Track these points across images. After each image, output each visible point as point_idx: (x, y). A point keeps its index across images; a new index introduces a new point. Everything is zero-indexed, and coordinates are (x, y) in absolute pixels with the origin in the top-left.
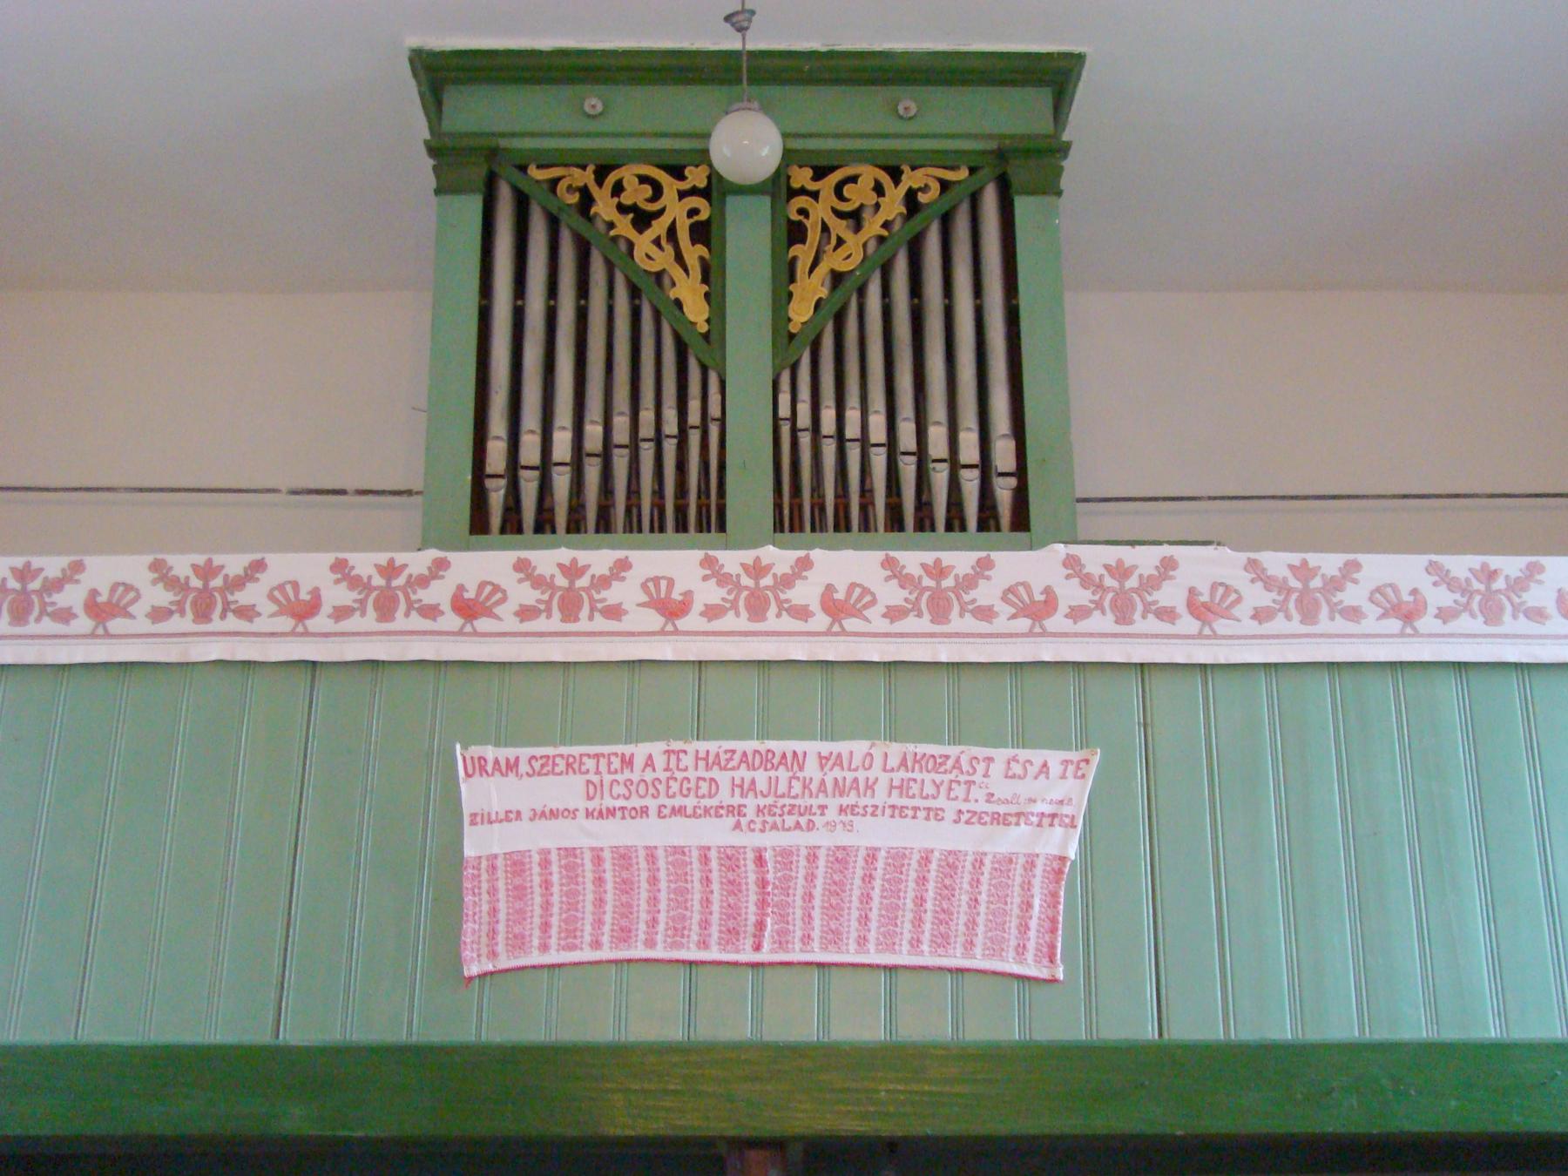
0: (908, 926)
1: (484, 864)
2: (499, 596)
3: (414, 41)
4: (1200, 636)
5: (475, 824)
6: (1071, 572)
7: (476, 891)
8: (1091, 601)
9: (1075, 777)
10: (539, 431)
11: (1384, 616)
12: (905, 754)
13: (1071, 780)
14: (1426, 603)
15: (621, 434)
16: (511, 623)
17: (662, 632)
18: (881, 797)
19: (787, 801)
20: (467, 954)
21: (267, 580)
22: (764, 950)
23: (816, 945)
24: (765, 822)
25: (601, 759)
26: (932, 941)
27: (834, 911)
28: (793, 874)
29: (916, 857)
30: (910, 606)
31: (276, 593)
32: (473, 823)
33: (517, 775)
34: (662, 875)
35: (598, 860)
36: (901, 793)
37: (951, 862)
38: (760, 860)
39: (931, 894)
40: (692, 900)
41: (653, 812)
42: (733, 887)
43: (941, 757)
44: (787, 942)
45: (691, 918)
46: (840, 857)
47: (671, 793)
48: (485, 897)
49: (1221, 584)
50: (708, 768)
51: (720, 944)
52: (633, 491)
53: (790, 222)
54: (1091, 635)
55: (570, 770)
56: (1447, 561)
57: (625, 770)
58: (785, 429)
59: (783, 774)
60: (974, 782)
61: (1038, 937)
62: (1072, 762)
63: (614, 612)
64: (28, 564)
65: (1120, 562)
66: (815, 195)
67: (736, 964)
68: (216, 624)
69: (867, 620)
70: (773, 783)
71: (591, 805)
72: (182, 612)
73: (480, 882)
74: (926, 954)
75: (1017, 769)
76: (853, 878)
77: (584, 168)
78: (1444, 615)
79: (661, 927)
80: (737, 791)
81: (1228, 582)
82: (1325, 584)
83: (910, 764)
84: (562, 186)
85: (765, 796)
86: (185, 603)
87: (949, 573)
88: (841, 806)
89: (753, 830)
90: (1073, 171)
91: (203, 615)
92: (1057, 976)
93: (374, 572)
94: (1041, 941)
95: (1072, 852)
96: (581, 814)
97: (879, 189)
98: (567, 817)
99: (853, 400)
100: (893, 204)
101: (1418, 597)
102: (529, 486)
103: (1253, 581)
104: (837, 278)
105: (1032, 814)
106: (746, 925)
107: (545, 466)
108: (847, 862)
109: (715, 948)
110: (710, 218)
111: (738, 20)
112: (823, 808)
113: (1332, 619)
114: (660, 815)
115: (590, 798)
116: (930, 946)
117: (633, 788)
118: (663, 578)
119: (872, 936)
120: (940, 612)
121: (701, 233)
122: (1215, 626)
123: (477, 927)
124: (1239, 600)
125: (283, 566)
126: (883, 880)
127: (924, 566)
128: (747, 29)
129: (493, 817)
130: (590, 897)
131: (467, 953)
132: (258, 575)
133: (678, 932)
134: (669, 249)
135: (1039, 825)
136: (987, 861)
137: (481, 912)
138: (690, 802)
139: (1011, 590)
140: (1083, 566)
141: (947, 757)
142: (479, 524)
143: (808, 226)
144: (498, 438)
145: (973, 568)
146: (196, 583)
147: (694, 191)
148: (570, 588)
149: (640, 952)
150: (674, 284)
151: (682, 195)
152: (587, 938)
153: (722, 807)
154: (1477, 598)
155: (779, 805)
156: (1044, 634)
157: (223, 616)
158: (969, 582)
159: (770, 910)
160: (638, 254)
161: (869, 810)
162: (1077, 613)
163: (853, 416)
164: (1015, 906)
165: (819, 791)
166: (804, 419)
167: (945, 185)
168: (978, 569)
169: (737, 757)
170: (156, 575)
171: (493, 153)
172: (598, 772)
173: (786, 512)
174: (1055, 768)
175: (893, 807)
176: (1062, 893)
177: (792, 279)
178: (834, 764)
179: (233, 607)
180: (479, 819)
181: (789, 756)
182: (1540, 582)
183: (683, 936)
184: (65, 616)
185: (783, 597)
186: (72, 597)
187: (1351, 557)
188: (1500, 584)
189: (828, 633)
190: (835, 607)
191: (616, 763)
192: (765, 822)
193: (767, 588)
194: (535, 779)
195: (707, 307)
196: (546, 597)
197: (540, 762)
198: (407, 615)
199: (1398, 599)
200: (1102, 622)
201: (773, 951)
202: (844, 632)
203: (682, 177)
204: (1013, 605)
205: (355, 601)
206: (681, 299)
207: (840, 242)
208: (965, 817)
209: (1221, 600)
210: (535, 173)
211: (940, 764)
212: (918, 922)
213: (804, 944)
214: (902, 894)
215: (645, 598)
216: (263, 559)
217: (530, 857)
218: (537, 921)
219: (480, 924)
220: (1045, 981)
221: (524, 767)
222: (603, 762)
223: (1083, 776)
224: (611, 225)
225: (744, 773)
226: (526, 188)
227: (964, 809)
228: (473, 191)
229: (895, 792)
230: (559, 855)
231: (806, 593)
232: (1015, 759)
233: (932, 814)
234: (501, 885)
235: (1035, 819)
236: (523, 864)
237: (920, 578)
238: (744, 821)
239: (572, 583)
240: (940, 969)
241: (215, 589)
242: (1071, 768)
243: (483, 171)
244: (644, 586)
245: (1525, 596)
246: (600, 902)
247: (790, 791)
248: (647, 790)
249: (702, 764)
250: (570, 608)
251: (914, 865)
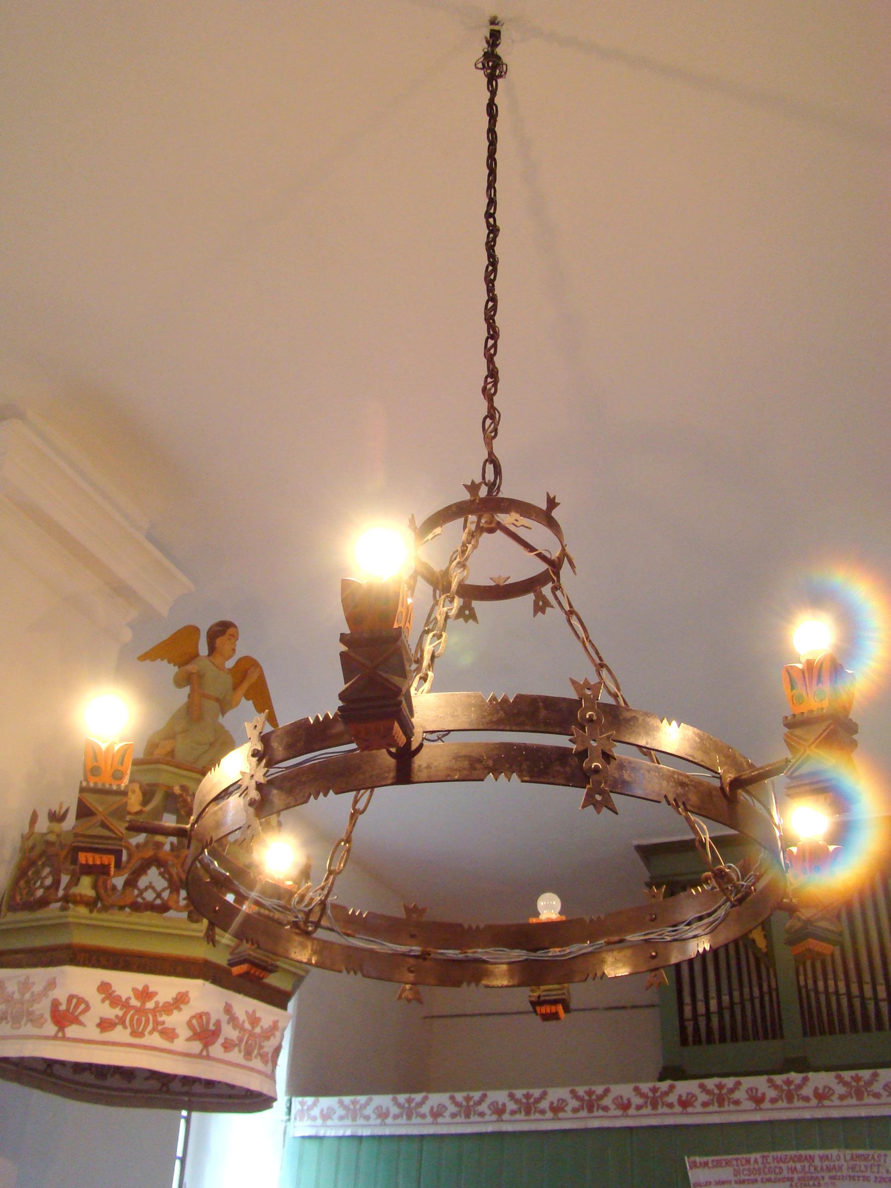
15: (737, 999)
19: (809, 1175)
24: (801, 1184)
50: (778, 1162)
63: (737, 1102)
68: (595, 1113)
69: (832, 1101)
70: (803, 1168)
71: (737, 1178)
80: (790, 1171)
91: (590, 1110)
96: (733, 1182)
112: (823, 1178)
114: (762, 1182)
120: (859, 1096)
127: (852, 1077)
138: (773, 1176)
141: (869, 1155)
158: (870, 1083)
175: (850, 1176)
181: (808, 1157)
191: (744, 1162)
192: (801, 1184)
202: (823, 1106)
221: (710, 1165)
222: (739, 1162)
225: (791, 1164)
231: (807, 1091)
238: (793, 1184)
244: (747, 1091)
250: (721, 1101)
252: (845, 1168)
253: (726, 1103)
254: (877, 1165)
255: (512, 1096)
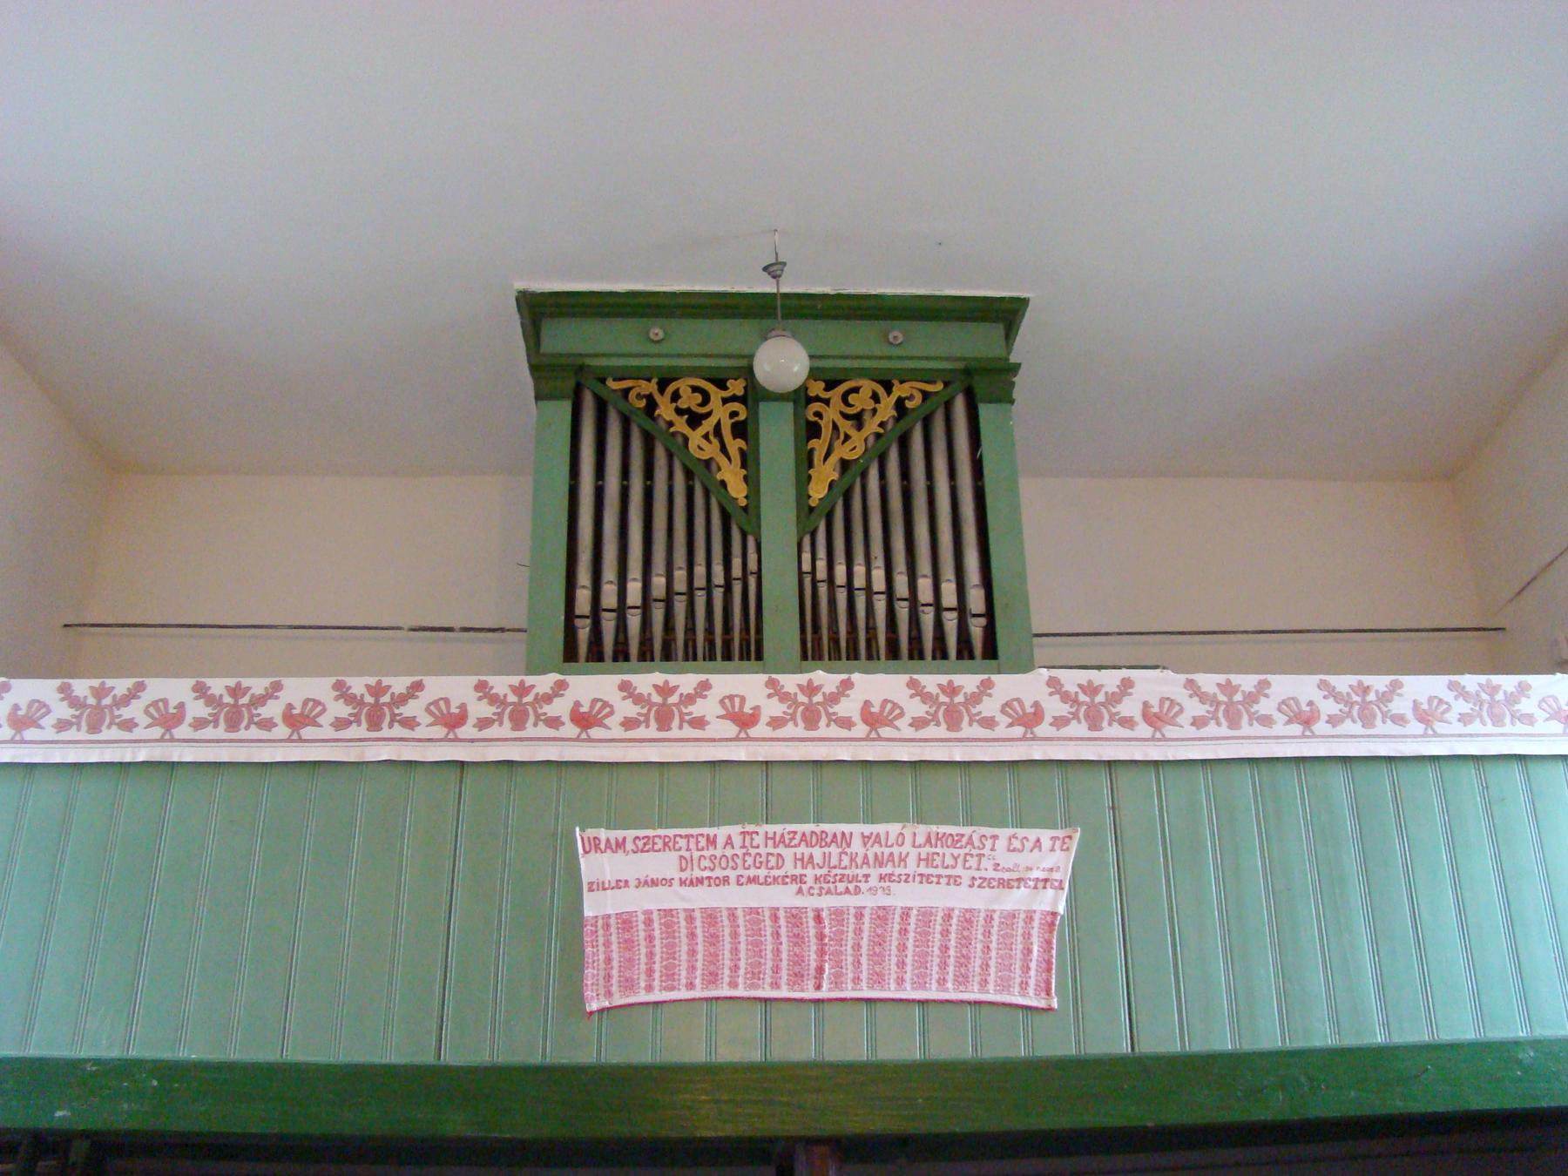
0: (936, 969)
1: (600, 922)
2: (608, 710)
3: (520, 285)
4: (1153, 739)
5: (593, 891)
6: (1053, 690)
7: (594, 943)
8: (1069, 713)
9: (1062, 850)
10: (616, 581)
11: (1290, 722)
12: (929, 833)
13: (1058, 852)
14: (1319, 711)
15: (680, 584)
16: (618, 732)
17: (737, 739)
18: (911, 867)
19: (839, 871)
20: (588, 993)
21: (425, 697)
22: (824, 989)
23: (864, 984)
24: (821, 888)
25: (691, 840)
26: (955, 980)
27: (877, 958)
28: (845, 929)
29: (941, 914)
30: (930, 718)
31: (432, 708)
32: (591, 890)
33: (624, 852)
34: (742, 930)
35: (690, 918)
36: (927, 864)
37: (968, 918)
38: (818, 919)
39: (953, 943)
40: (766, 950)
41: (733, 880)
42: (798, 939)
43: (957, 835)
44: (842, 983)
45: (765, 964)
46: (881, 914)
47: (746, 865)
48: (602, 949)
49: (1168, 699)
50: (775, 846)
51: (789, 985)
52: (690, 629)
53: (808, 422)
54: (1071, 739)
55: (667, 848)
56: (1333, 680)
57: (710, 848)
58: (808, 580)
59: (834, 850)
60: (984, 855)
61: (1037, 976)
62: (1058, 838)
63: (699, 723)
64: (239, 684)
65: (1090, 682)
66: (827, 402)
67: (802, 1000)
68: (386, 732)
70: (826, 857)
71: (684, 875)
72: (359, 723)
73: (597, 936)
74: (951, 990)
75: (1016, 844)
76: (891, 932)
77: (649, 380)
78: (1333, 721)
79: (742, 972)
80: (799, 864)
81: (1173, 698)
82: (1245, 698)
83: (933, 841)
84: (632, 395)
85: (821, 868)
86: (361, 715)
87: (960, 691)
88: (881, 875)
89: (812, 895)
90: (1022, 386)
91: (375, 724)
92: (1053, 1006)
93: (508, 691)
94: (1040, 978)
95: (1061, 908)
96: (676, 883)
97: (875, 397)
98: (665, 885)
99: (859, 557)
100: (887, 410)
101: (1314, 707)
102: (609, 624)
103: (1191, 696)
104: (845, 465)
105: (1030, 879)
106: (808, 970)
107: (622, 609)
108: (887, 919)
109: (784, 987)
110: (746, 419)
111: (773, 270)
112: (867, 876)
113: (1251, 725)
114: (739, 884)
115: (682, 870)
116: (953, 984)
117: (717, 862)
118: (737, 696)
119: (908, 977)
120: (953, 721)
121: (740, 430)
122: (1164, 731)
123: (595, 972)
124: (1181, 711)
125: (437, 686)
126: (915, 932)
127: (940, 686)
128: (780, 276)
129: (607, 886)
130: (685, 948)
131: (589, 993)
132: (417, 693)
133: (755, 975)
134: (715, 441)
135: (1035, 888)
136: (996, 916)
137: (598, 960)
138: (762, 873)
139: (1007, 704)
140: (1062, 686)
141: (963, 835)
142: (570, 654)
143: (822, 425)
144: (584, 587)
145: (978, 687)
146: (369, 699)
147: (734, 399)
148: (664, 704)
149: (726, 992)
150: (719, 469)
151: (725, 401)
152: (684, 981)
153: (787, 877)
154: (1357, 707)
155: (832, 874)
156: (1035, 738)
157: (391, 726)
158: (975, 699)
159: (827, 957)
160: (692, 446)
161: (903, 878)
162: (1059, 722)
163: (859, 570)
164: (1018, 952)
165: (864, 863)
166: (822, 573)
167: (926, 395)
168: (982, 689)
169: (798, 837)
170: (338, 693)
171: (581, 369)
172: (688, 849)
173: (809, 645)
174: (1046, 843)
175: (921, 875)
176: (1054, 941)
177: (811, 465)
178: (875, 842)
179: (398, 718)
180: (595, 887)
182: (1400, 695)
183: (759, 979)
184: (267, 724)
185: (831, 710)
186: (273, 710)
187: (1262, 677)
188: (1371, 697)
189: (867, 739)
190: (874, 719)
192: (821, 888)
193: (818, 703)
194: (639, 854)
195: (745, 486)
196: (645, 711)
197: (642, 841)
198: (535, 725)
199: (1298, 708)
200: (1078, 729)
201: (830, 990)
202: (880, 739)
203: (725, 388)
204: (1009, 716)
205: (494, 714)
206: (726, 479)
207: (847, 437)
208: (977, 882)
209: (1168, 710)
210: (614, 385)
211: (957, 840)
212: (943, 965)
213: (855, 984)
214: (930, 944)
215: (723, 712)
216: (421, 680)
217: (636, 916)
218: (643, 967)
219: (598, 970)
220: (1043, 1009)
221: (629, 846)
222: (692, 841)
223: (1068, 849)
224: (671, 424)
225: (803, 849)
226: (604, 394)
227: (977, 876)
228: (562, 397)
229: (923, 864)
230: (659, 914)
231: (849, 707)
232: (1014, 836)
233: (952, 880)
234: (614, 938)
235: (1031, 883)
236: (631, 922)
237: (937, 695)
238: (805, 887)
239: (665, 700)
240: (962, 1002)
241: (384, 704)
242: (1058, 843)
243: (572, 383)
244: (722, 702)
245: (1391, 706)
246: (692, 952)
247: (840, 864)
248: (728, 862)
249: (770, 843)
250: (664, 721)
251: (939, 920)
252: (911, 861)
253: (676, 722)
254: (977, 856)
255: (201, 691)
